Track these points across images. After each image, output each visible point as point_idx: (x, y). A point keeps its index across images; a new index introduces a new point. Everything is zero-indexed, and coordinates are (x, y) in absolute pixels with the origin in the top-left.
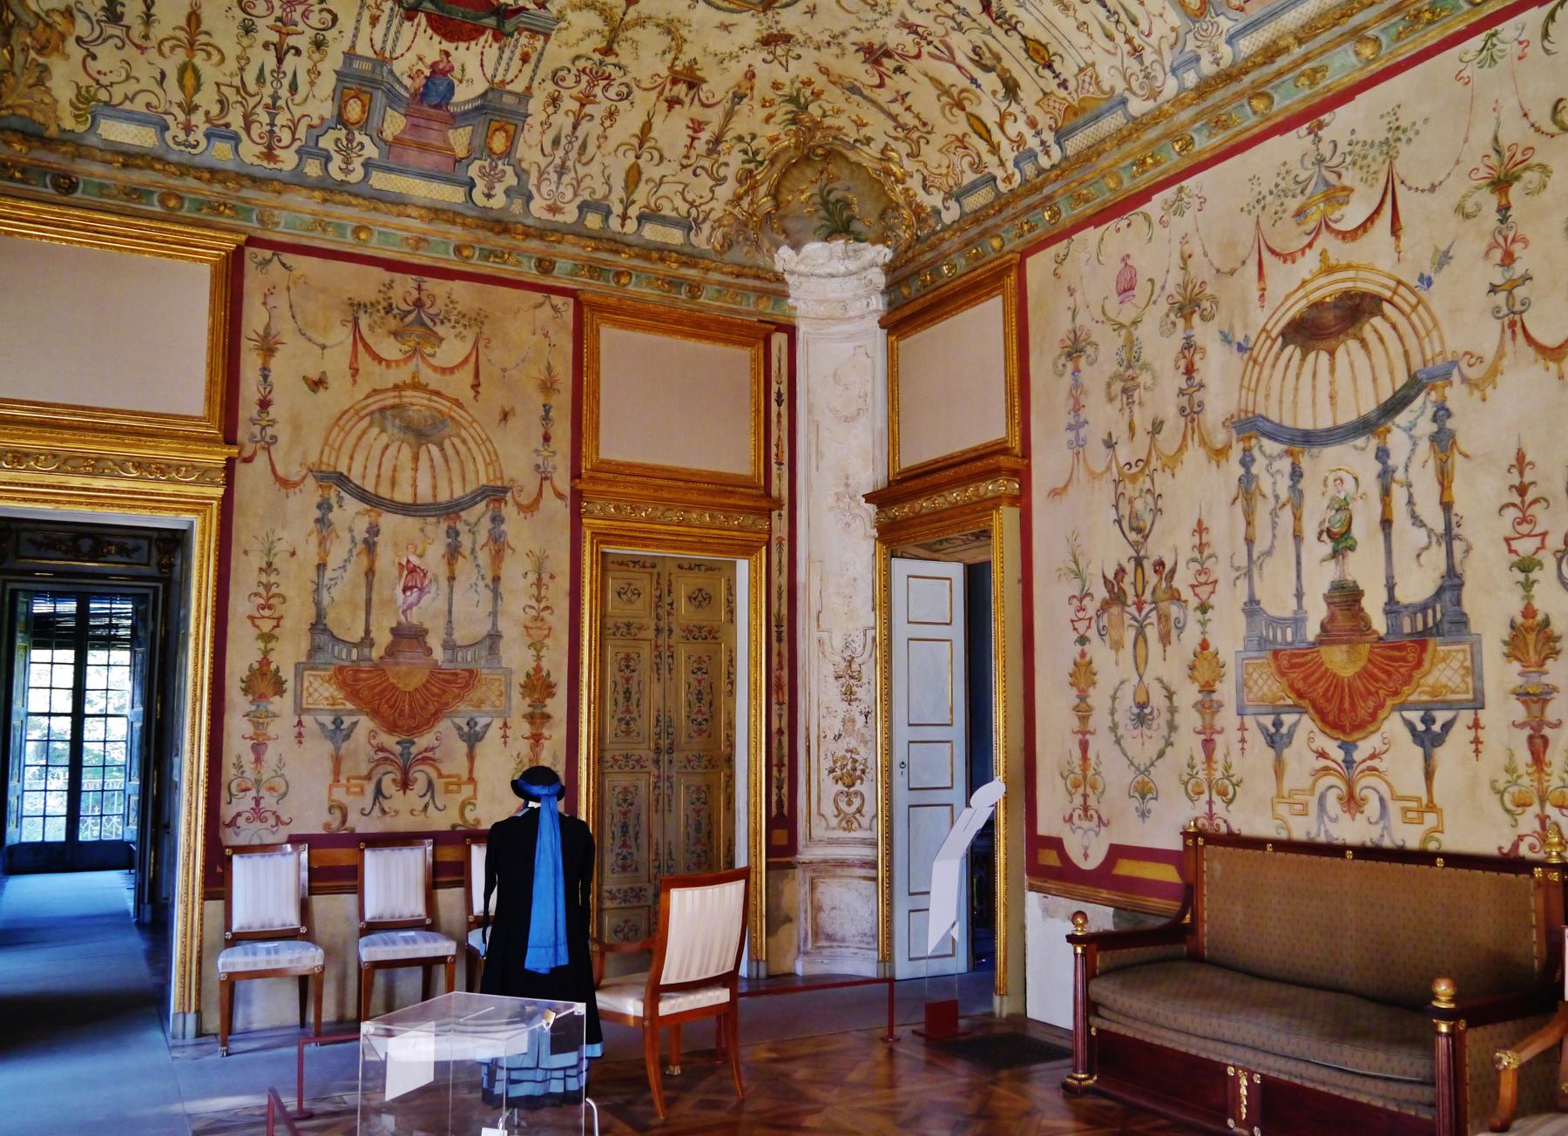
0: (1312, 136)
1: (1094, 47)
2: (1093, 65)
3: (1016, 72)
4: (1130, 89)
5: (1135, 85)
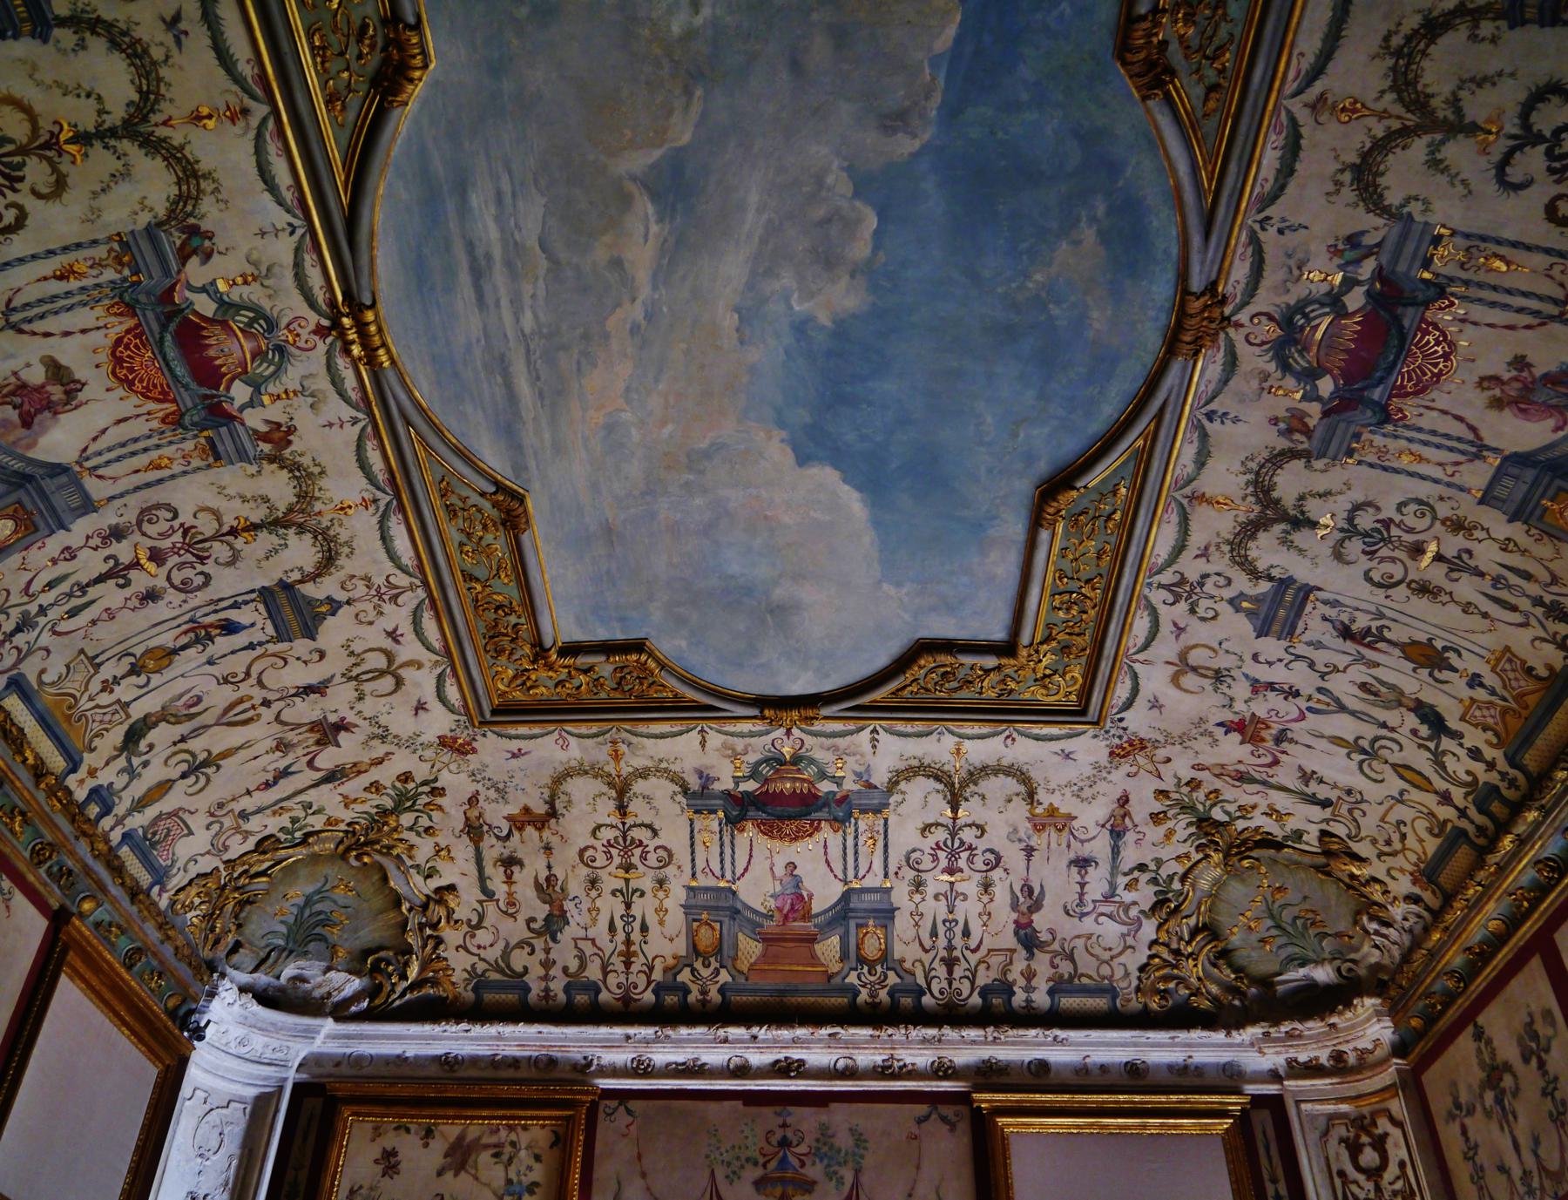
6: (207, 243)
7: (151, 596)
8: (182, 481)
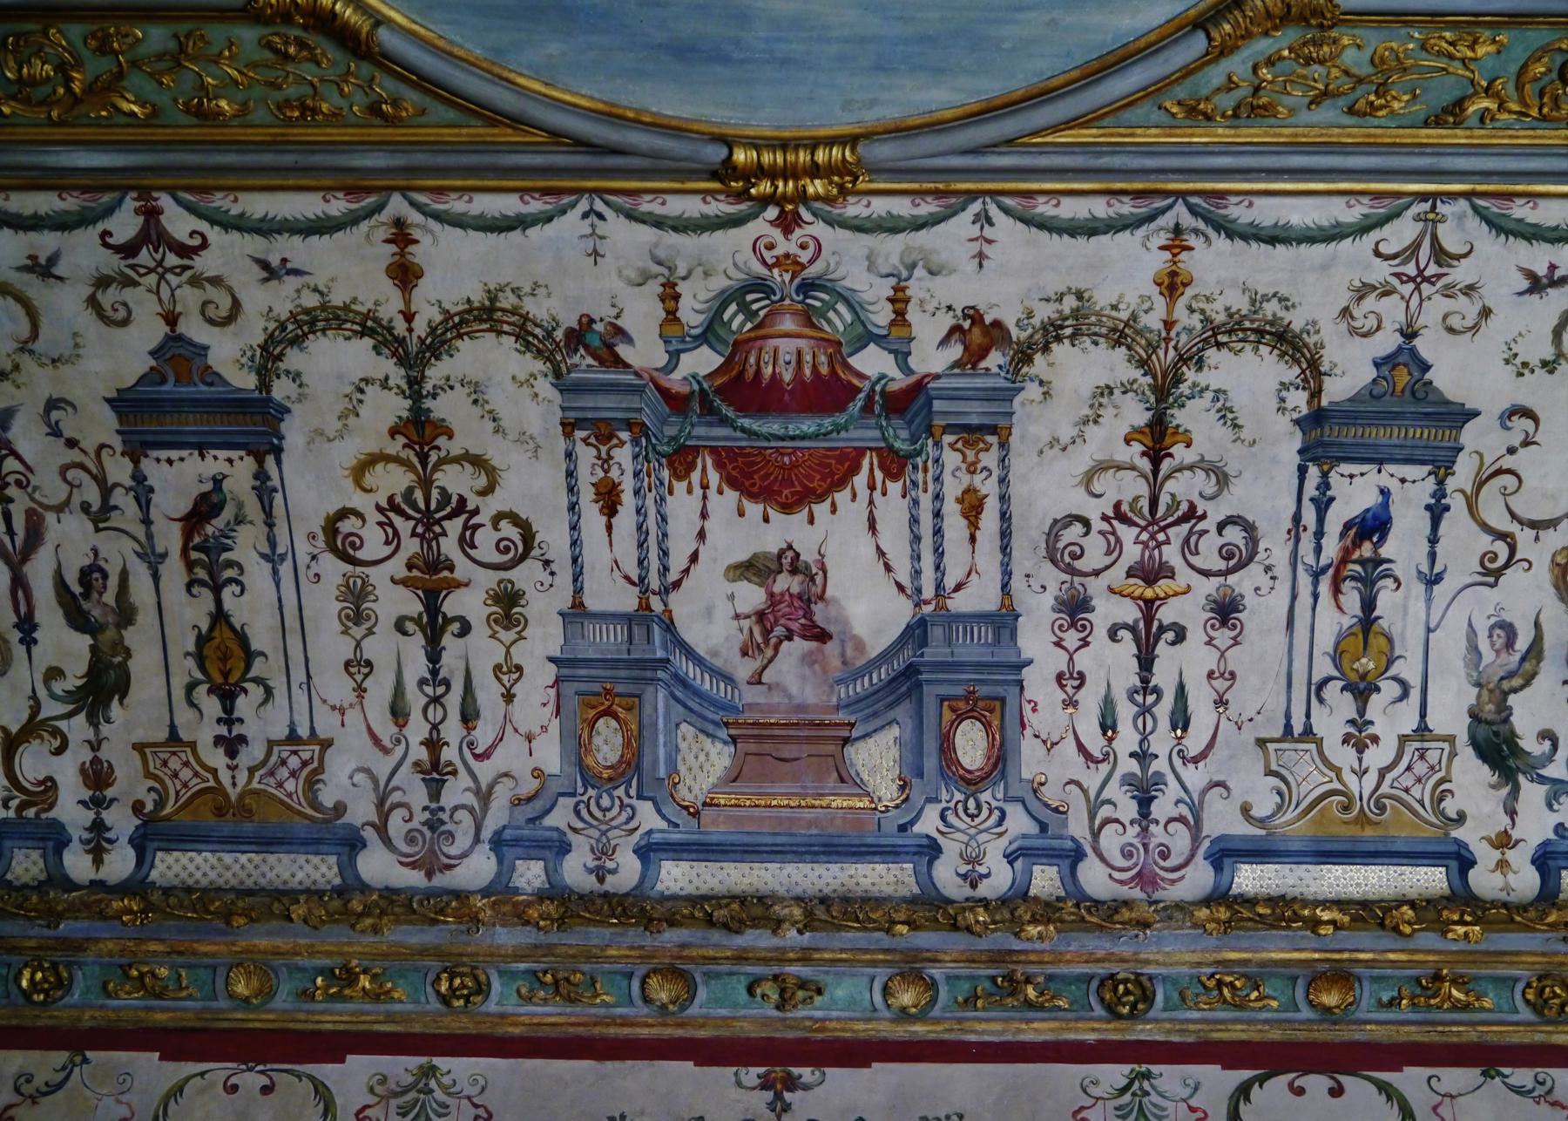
0: (769, 1095)
1: (353, 716)
2: (326, 744)
3: (144, 663)
4: (382, 830)
5: (397, 825)
6: (599, 327)
7: (1226, 611)
8: (1016, 489)
